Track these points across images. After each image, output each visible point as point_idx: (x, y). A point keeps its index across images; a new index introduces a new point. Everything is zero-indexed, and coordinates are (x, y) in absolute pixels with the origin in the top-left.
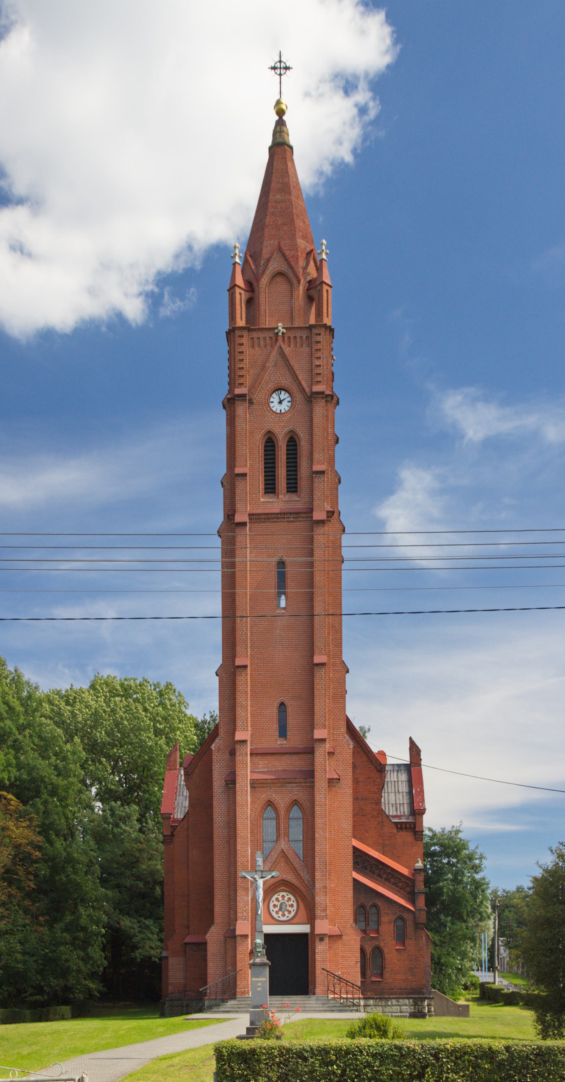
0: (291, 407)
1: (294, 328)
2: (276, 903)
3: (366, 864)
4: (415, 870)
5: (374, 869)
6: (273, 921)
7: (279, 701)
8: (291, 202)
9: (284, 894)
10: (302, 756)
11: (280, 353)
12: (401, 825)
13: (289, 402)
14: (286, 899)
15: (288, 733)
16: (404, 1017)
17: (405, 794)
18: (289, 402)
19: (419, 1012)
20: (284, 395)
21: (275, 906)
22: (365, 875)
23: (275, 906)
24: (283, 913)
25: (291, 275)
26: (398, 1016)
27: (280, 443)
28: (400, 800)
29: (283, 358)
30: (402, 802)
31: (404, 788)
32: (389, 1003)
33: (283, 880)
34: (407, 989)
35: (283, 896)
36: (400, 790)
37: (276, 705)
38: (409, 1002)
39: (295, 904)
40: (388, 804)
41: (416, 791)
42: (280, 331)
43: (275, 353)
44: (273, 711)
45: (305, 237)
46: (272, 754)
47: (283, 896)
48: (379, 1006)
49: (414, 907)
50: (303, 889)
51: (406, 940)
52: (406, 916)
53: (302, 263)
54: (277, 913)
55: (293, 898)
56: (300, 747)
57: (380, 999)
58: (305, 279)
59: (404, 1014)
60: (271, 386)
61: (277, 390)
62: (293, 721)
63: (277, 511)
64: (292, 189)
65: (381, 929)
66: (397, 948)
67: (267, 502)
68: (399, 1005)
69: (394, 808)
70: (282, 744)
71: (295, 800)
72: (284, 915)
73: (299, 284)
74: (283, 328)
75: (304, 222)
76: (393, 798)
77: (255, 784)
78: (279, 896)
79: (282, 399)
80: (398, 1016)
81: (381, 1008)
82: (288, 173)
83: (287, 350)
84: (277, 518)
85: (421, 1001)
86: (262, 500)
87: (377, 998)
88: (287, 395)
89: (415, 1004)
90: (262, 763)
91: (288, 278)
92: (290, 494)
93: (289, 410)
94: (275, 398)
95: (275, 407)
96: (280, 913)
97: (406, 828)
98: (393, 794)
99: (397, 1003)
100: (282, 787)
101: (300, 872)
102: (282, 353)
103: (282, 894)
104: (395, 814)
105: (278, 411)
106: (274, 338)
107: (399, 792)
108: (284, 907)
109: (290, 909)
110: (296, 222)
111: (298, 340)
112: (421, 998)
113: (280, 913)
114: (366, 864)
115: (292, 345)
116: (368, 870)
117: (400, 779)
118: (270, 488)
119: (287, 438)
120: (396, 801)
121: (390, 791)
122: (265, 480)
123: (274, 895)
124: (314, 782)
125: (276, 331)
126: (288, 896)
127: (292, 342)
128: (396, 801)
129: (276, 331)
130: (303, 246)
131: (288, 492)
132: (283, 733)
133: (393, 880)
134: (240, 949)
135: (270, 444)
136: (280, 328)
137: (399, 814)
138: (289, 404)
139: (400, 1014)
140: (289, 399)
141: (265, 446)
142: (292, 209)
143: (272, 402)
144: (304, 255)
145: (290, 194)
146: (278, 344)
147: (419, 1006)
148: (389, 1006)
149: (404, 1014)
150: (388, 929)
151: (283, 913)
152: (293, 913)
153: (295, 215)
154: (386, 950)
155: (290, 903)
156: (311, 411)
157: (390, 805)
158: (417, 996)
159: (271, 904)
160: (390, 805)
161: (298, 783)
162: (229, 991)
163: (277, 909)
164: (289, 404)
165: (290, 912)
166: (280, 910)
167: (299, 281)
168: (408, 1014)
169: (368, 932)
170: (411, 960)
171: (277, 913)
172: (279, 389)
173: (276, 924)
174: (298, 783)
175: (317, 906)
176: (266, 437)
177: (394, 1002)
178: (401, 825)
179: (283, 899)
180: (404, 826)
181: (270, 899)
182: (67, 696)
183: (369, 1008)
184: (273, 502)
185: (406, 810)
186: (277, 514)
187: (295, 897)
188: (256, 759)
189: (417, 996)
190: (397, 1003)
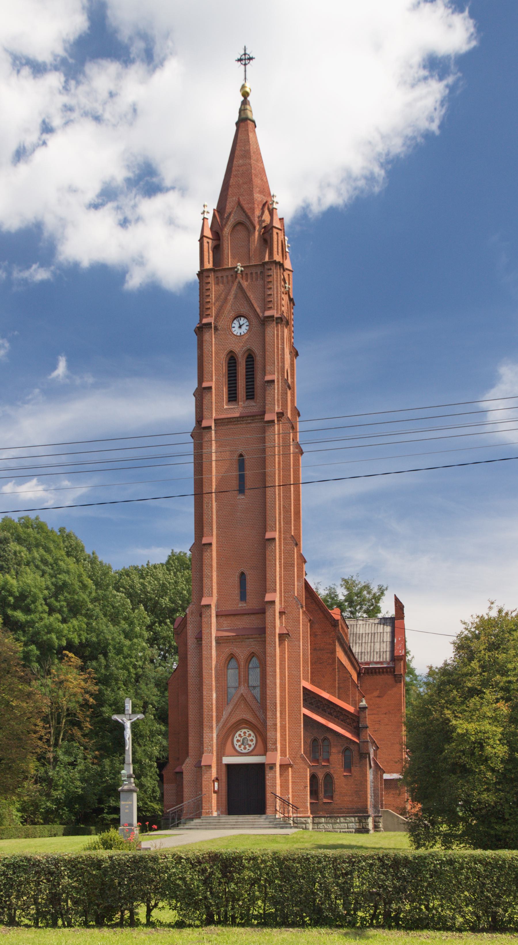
0: (248, 330)
1: (250, 266)
2: (239, 738)
3: (319, 704)
4: (360, 708)
5: (325, 708)
7: (240, 571)
8: (251, 165)
9: (246, 730)
10: (258, 615)
11: (239, 287)
12: (383, 670)
13: (247, 326)
14: (247, 735)
15: (247, 597)
16: (351, 832)
17: (388, 643)
18: (247, 326)
19: (363, 828)
20: (243, 321)
21: (238, 741)
22: (318, 714)
23: (238, 741)
24: (245, 746)
25: (248, 223)
26: (343, 832)
27: (240, 360)
28: (383, 648)
29: (242, 291)
30: (385, 650)
31: (387, 638)
32: (338, 821)
33: (243, 719)
34: (353, 808)
35: (245, 733)
36: (385, 640)
37: (237, 574)
38: (355, 820)
39: (254, 739)
40: (374, 652)
41: (397, 640)
42: (238, 269)
44: (236, 580)
45: (261, 192)
46: (234, 615)
47: (245, 733)
48: (329, 823)
49: (359, 739)
50: (259, 726)
51: (352, 768)
52: (352, 747)
53: (257, 213)
54: (240, 746)
55: (252, 734)
56: (257, 608)
57: (330, 817)
59: (351, 830)
60: (232, 314)
61: (237, 317)
63: (237, 415)
64: (252, 154)
65: (331, 758)
66: (345, 774)
67: (229, 408)
68: (346, 823)
69: (378, 656)
70: (242, 607)
71: (253, 653)
72: (245, 748)
74: (241, 267)
75: (262, 180)
76: (378, 647)
77: (219, 640)
78: (241, 732)
79: (241, 324)
80: (345, 832)
81: (331, 825)
82: (249, 142)
83: (245, 284)
84: (238, 421)
85: (365, 819)
86: (225, 407)
87: (328, 817)
88: (246, 320)
89: (360, 822)
90: (226, 623)
91: (246, 226)
92: (248, 401)
93: (247, 333)
94: (236, 324)
95: (236, 331)
96: (243, 746)
97: (387, 672)
98: (378, 644)
99: (344, 821)
100: (242, 642)
102: (240, 287)
103: (243, 730)
104: (378, 660)
105: (239, 334)
106: (234, 276)
107: (383, 642)
108: (245, 741)
109: (250, 743)
110: (254, 181)
111: (254, 275)
112: (365, 816)
113: (243, 746)
114: (319, 704)
115: (249, 280)
116: (321, 709)
117: (385, 631)
118: (232, 397)
119: (246, 355)
120: (380, 649)
121: (376, 641)
122: (229, 391)
123: (237, 732)
124: (265, 637)
125: (236, 270)
126: (249, 732)
127: (249, 277)
128: (380, 649)
129: (236, 270)
130: (259, 199)
131: (247, 399)
132: (243, 597)
133: (342, 717)
134: (205, 777)
135: (232, 360)
136: (239, 267)
137: (381, 660)
138: (247, 328)
139: (347, 830)
140: (247, 324)
141: (229, 363)
142: (251, 170)
143: (234, 327)
144: (261, 207)
145: (250, 158)
146: (237, 280)
147: (363, 823)
148: (338, 823)
149: (351, 830)
150: (336, 758)
151: (245, 746)
152: (253, 747)
153: (253, 176)
154: (335, 776)
157: (375, 653)
158: (361, 815)
159: (235, 740)
160: (375, 653)
161: (254, 638)
162: (197, 812)
163: (239, 743)
164: (247, 328)
165: (250, 746)
166: (243, 744)
167: (254, 228)
168: (354, 830)
169: (320, 761)
170: (356, 785)
171: (240, 746)
172: (238, 316)
173: (238, 756)
174: (254, 638)
175: (268, 740)
176: (229, 356)
177: (342, 820)
178: (383, 670)
179: (245, 735)
180: (385, 670)
181: (234, 735)
182: (142, 571)
183: (321, 825)
184: (234, 408)
185: (387, 657)
186: (237, 418)
187: (254, 733)
188: (222, 620)
189: (361, 815)
190: (344, 821)
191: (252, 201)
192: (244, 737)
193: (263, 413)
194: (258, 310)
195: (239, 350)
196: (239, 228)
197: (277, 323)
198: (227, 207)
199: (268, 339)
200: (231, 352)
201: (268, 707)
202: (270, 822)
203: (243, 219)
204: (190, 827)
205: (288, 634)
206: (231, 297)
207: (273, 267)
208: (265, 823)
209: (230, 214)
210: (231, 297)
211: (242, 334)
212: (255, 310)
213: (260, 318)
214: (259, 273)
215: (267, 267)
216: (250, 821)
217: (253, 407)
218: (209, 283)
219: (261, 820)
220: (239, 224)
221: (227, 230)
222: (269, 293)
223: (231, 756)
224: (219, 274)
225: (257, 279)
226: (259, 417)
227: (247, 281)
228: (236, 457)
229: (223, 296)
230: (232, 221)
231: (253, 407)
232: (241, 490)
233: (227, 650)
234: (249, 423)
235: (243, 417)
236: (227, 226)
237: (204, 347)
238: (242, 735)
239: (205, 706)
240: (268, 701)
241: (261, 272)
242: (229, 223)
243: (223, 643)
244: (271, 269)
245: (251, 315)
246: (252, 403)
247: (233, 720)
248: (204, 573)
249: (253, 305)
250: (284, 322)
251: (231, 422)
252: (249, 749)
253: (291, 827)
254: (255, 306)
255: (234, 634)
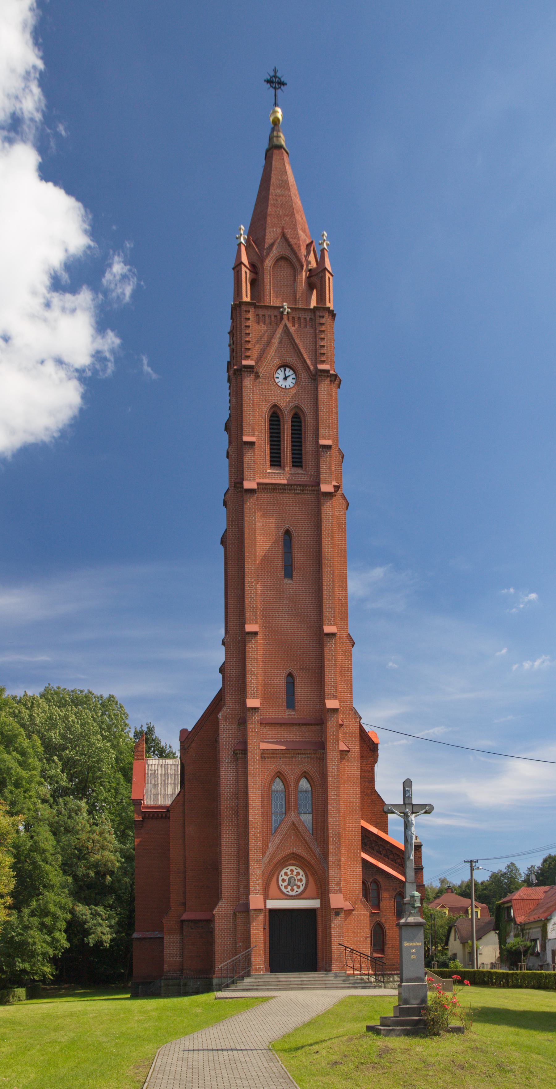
0: (296, 384)
6: (286, 897)
7: (287, 671)
9: (293, 868)
10: (311, 727)
11: (285, 331)
13: (293, 379)
14: (295, 873)
15: (297, 704)
18: (293, 379)
20: (289, 372)
21: (284, 880)
23: (284, 880)
24: (292, 887)
25: (294, 260)
27: (286, 417)
29: (288, 336)
33: (293, 853)
39: (304, 879)
43: (281, 331)
47: (292, 871)
55: (301, 872)
58: (307, 266)
60: (277, 362)
62: (300, 691)
63: (284, 482)
70: (290, 715)
71: (305, 772)
72: (292, 890)
73: (303, 269)
74: (288, 308)
79: (287, 375)
83: (292, 329)
86: (268, 471)
88: (291, 372)
91: (291, 263)
93: (294, 387)
96: (289, 887)
100: (292, 757)
101: (311, 845)
103: (290, 868)
106: (279, 317)
108: (292, 881)
109: (299, 883)
111: (302, 321)
113: (289, 887)
115: (296, 325)
118: (276, 461)
119: (292, 414)
123: (283, 869)
125: (282, 310)
129: (282, 310)
131: (293, 466)
132: (291, 704)
135: (275, 418)
138: (294, 381)
140: (294, 376)
143: (278, 378)
146: (283, 322)
151: (292, 887)
152: (302, 888)
155: (299, 877)
156: (316, 390)
159: (280, 879)
163: (286, 883)
164: (294, 381)
166: (289, 884)
167: (302, 266)
171: (286, 887)
172: (284, 366)
173: (286, 899)
176: (272, 411)
186: (284, 485)
187: (304, 871)
191: (297, 237)
192: (293, 875)
193: (318, 484)
194: (308, 361)
195: (285, 404)
196: (282, 263)
197: (331, 381)
198: (267, 237)
199: (321, 397)
200: (275, 406)
201: (331, 839)
202: (344, 981)
203: (288, 253)
204: (244, 988)
205: (348, 751)
206: (276, 341)
207: (326, 315)
208: (337, 982)
209: (272, 245)
210: (276, 341)
211: (288, 387)
212: (305, 362)
213: (311, 372)
214: (308, 319)
215: (318, 313)
216: (317, 979)
217: (303, 476)
218: (249, 319)
219: (330, 979)
220: (282, 258)
221: (269, 263)
222: (322, 344)
223: (276, 899)
224: (261, 312)
225: (306, 326)
226: (310, 488)
227: (294, 326)
228: (282, 532)
229: (265, 338)
230: (275, 252)
231: (303, 476)
232: (288, 572)
233: (273, 768)
234: (298, 494)
235: (291, 485)
236: (269, 258)
237: (244, 394)
238: (289, 873)
239: (251, 835)
240: (330, 831)
241: (311, 319)
242: (271, 255)
243: (268, 758)
244: (323, 317)
245: (299, 366)
246: (299, 471)
247: (281, 855)
248: (248, 668)
249: (302, 355)
250: (337, 382)
251: (276, 489)
252: (297, 891)
253: (375, 987)
254: (305, 356)
255: (284, 748)
